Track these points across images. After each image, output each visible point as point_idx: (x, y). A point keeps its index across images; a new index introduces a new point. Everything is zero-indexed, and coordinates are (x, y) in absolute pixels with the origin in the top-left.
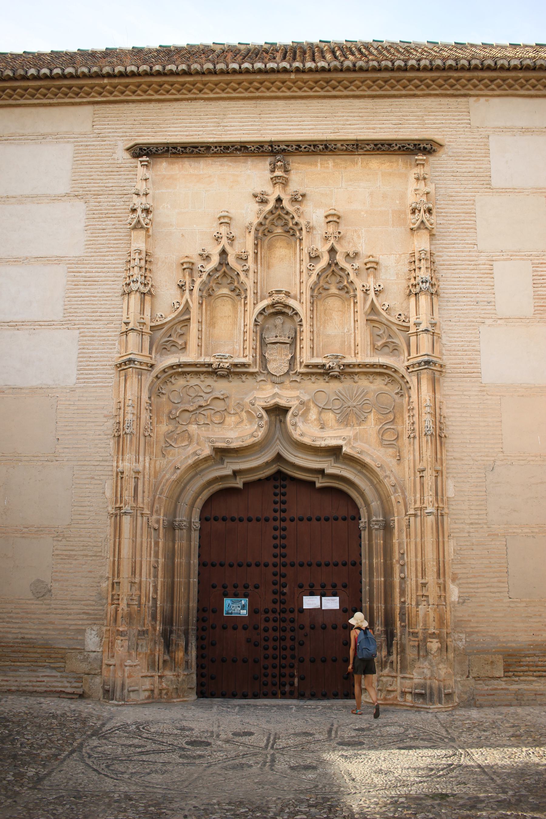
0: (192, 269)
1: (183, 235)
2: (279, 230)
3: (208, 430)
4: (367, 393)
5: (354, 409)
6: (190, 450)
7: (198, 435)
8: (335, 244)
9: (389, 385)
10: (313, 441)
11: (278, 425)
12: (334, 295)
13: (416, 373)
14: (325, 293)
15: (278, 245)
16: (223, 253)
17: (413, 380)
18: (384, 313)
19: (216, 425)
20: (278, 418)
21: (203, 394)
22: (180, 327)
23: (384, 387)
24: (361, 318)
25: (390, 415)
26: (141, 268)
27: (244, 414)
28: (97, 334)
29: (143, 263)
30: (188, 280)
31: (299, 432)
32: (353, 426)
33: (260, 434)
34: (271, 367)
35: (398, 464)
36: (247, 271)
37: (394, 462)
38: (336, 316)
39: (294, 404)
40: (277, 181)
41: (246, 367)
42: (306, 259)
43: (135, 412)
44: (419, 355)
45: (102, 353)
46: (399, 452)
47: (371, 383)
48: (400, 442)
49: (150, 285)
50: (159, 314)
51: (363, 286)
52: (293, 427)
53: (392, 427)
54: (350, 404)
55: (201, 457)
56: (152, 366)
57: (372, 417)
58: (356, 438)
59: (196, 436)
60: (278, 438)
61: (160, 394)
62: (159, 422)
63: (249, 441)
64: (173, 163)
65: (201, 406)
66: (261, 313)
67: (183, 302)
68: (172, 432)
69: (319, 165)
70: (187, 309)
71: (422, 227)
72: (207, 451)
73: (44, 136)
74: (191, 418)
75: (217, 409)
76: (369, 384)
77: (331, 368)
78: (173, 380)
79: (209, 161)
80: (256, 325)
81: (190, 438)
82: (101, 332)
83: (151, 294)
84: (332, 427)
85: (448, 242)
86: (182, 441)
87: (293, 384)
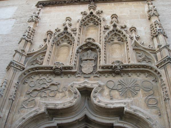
0: (51, 35)
1: (50, 25)
2: (91, 24)
3: (46, 100)
4: (136, 81)
5: (130, 89)
6: (34, 109)
7: (40, 102)
8: (115, 23)
9: (148, 77)
10: (106, 105)
11: (86, 100)
12: (116, 43)
13: (163, 67)
14: (112, 42)
15: (91, 29)
16: (66, 29)
17: (162, 71)
18: (142, 45)
19: (51, 98)
20: (87, 97)
21: (46, 83)
22: (41, 56)
23: (145, 78)
24: (131, 49)
25: (150, 92)
26: (29, 33)
27: (67, 92)
28: (4, 58)
29: (30, 31)
30: (48, 37)
31: (97, 100)
32: (130, 98)
33: (74, 102)
34: (84, 70)
35: (160, 118)
36: (76, 33)
37: (157, 116)
38: (118, 51)
39: (95, 86)
40: (91, 8)
41: (70, 69)
42: (103, 29)
43: (7, 86)
44: (163, 58)
45: (3, 65)
46: (159, 111)
47: (138, 76)
48: (159, 106)
49: (31, 39)
50: (32, 49)
51: (130, 36)
52: (95, 98)
53: (153, 97)
54: (127, 86)
55: (39, 113)
56: (24, 69)
57: (140, 93)
58: (132, 103)
59: (38, 103)
60: (86, 107)
61: (25, 83)
62: (21, 96)
63: (68, 105)
64: (52, 8)
65: (44, 88)
66: (80, 48)
67: (45, 44)
68: (26, 100)
69: (108, 5)
70: (46, 47)
71: (154, 15)
72: (43, 110)
73: (9, 6)
74: (38, 94)
75: (52, 90)
76: (137, 77)
77: (116, 67)
78: (33, 77)
79: (65, 6)
80: (78, 53)
81: (35, 104)
82: (6, 58)
83: (31, 43)
84: (117, 99)
85: (166, 23)
86: (31, 105)
87: (96, 78)
